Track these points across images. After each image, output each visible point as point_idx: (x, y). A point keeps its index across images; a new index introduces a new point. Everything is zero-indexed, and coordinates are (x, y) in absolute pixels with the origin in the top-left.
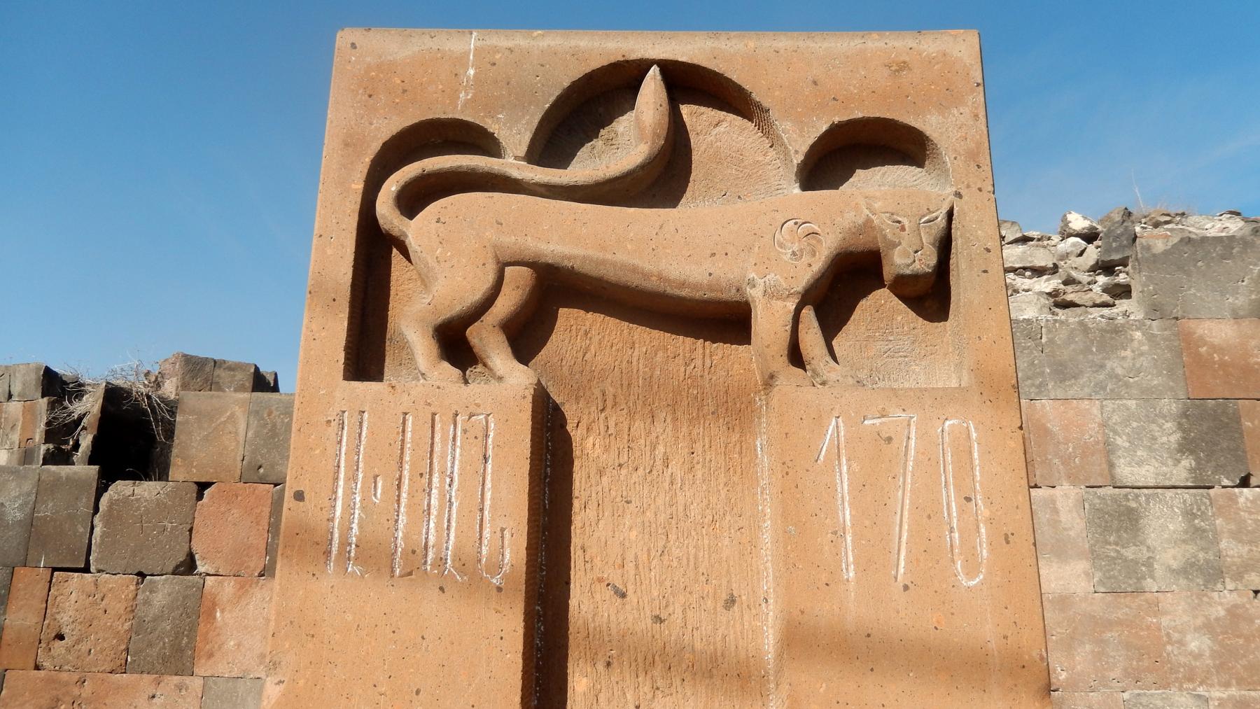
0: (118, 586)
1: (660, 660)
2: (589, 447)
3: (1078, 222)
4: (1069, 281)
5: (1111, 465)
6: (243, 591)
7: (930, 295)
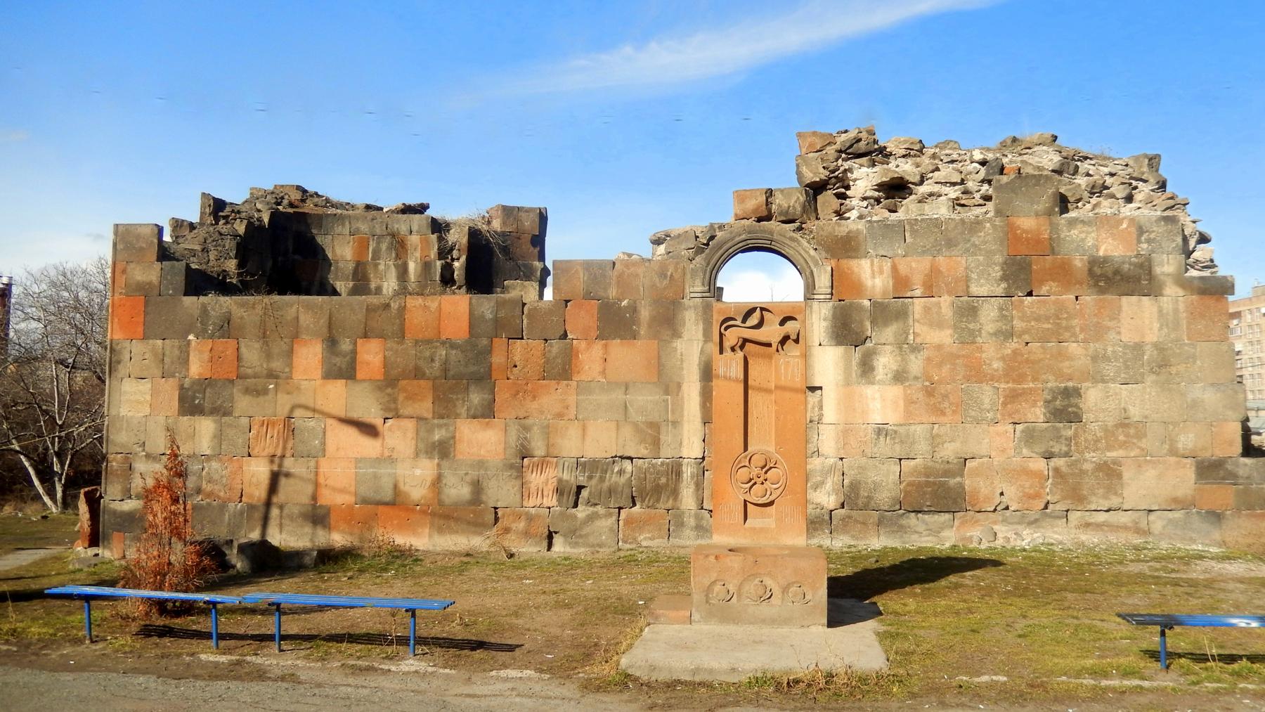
0: (539, 344)
1: (760, 389)
2: (750, 362)
3: (978, 156)
4: (965, 192)
5: (968, 287)
6: (589, 346)
7: (797, 341)
